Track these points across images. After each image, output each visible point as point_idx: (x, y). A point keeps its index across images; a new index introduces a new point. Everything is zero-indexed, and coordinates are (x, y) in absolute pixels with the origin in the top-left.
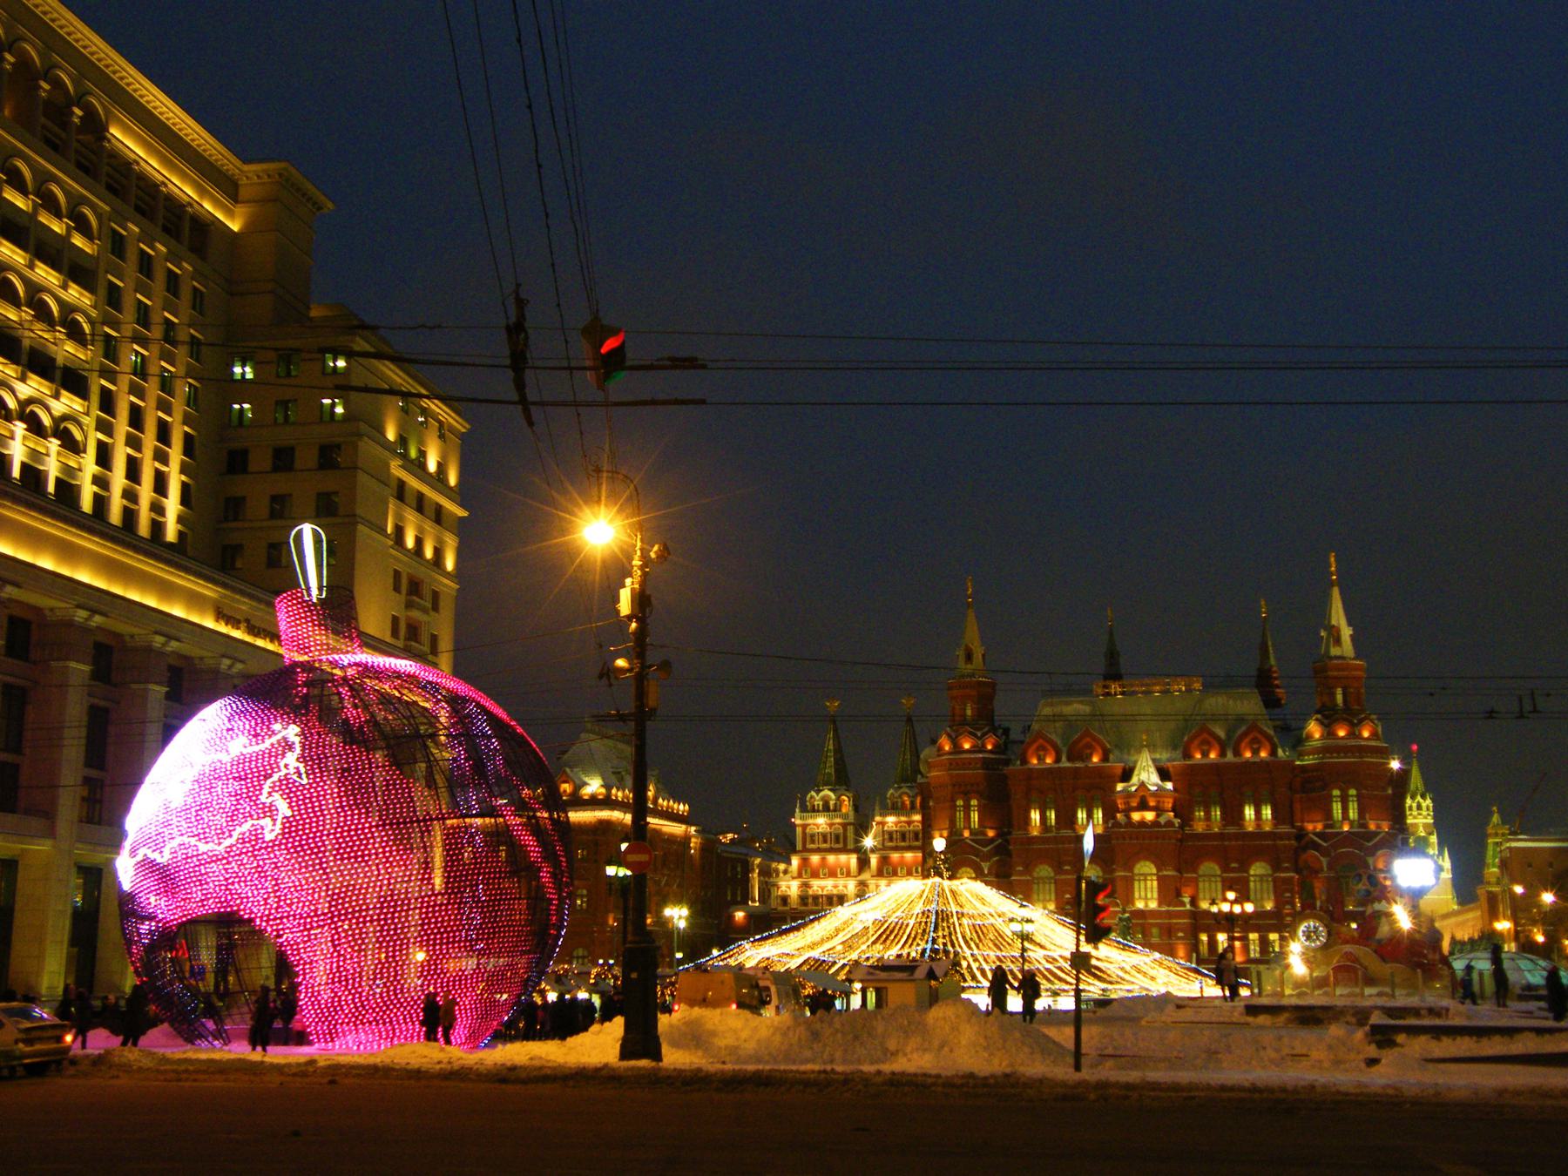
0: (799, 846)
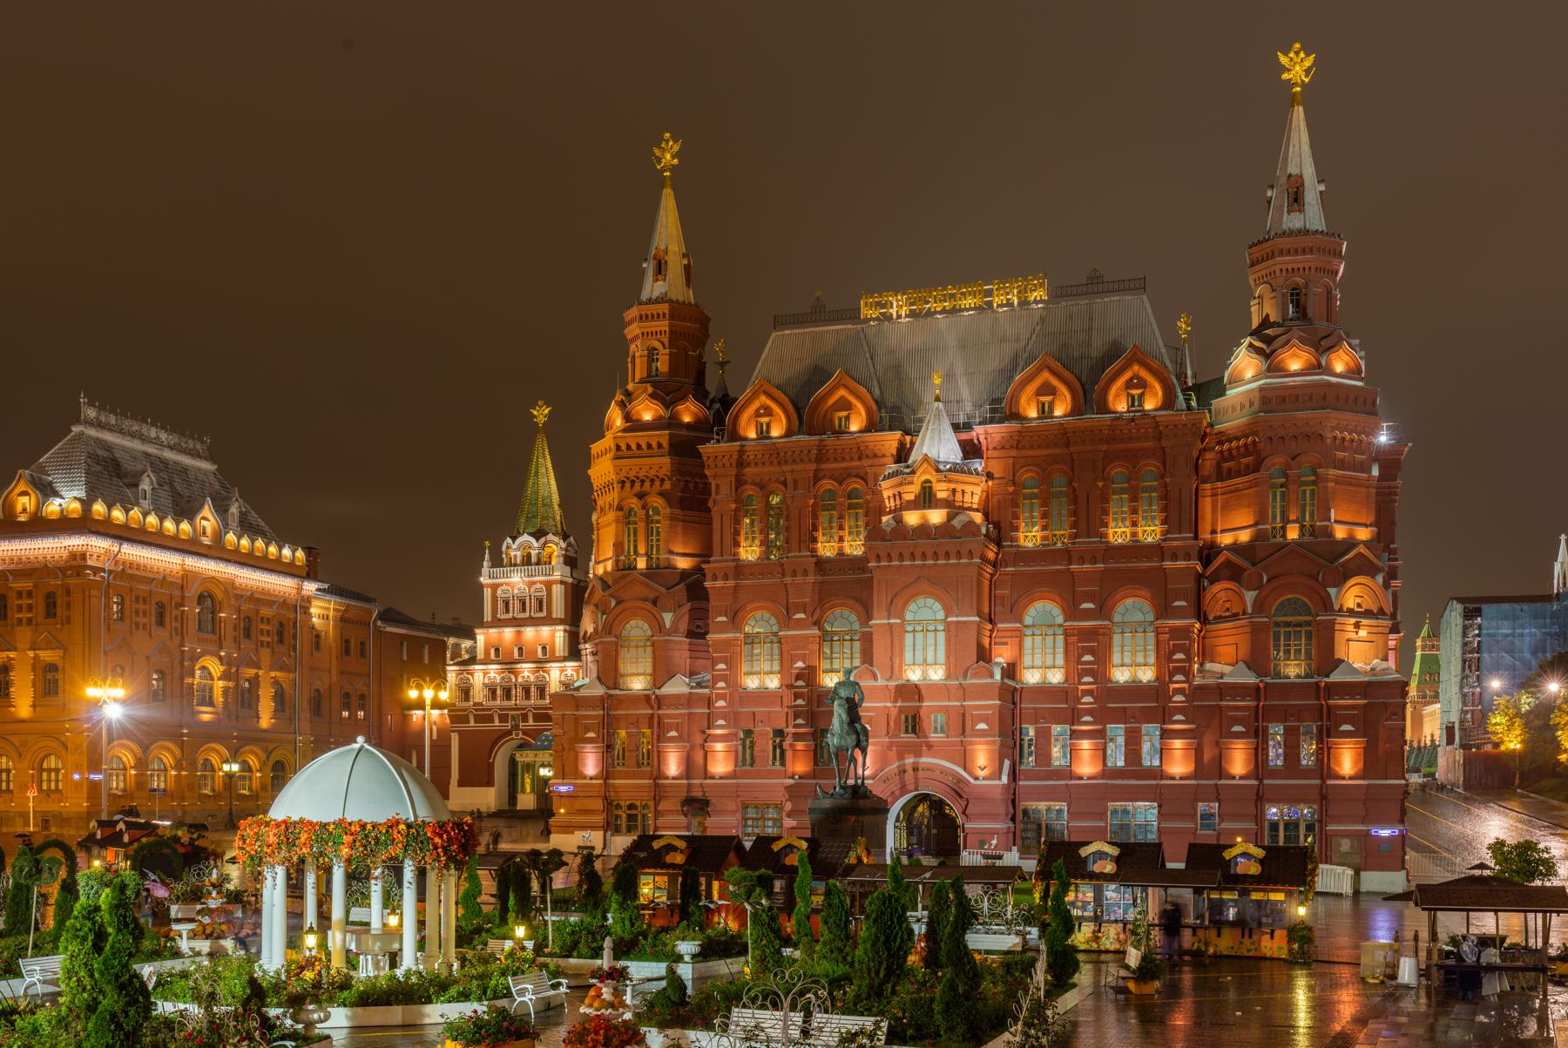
0: (488, 616)
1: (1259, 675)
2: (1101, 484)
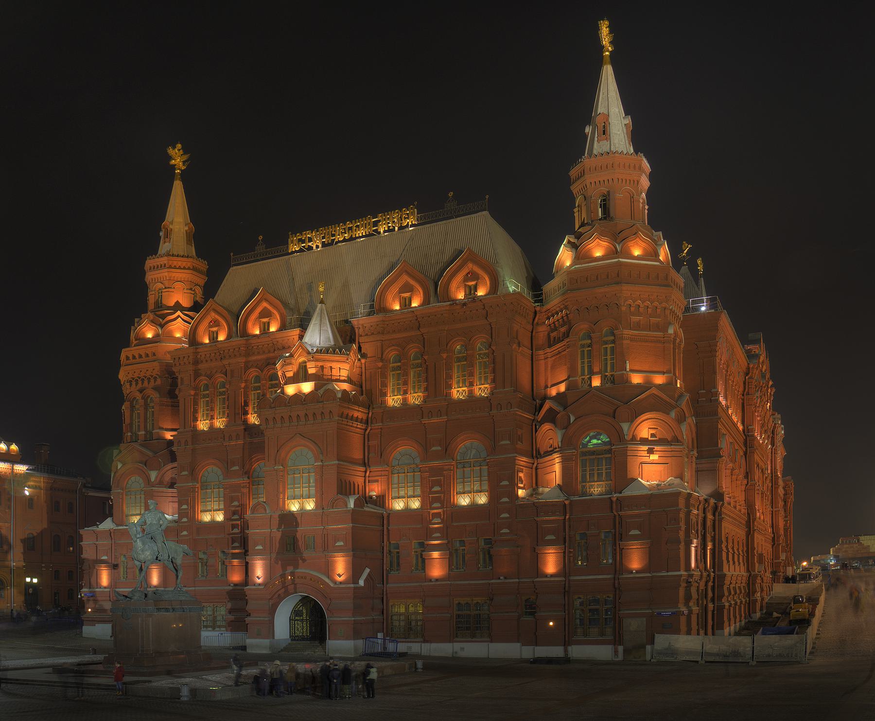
2: (445, 356)
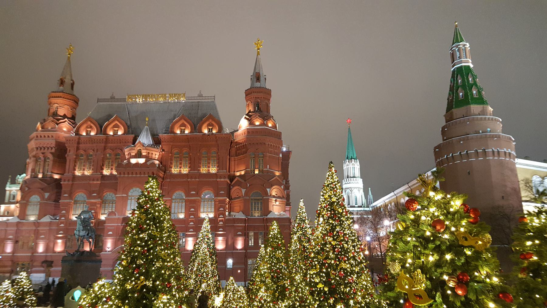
1: (246, 216)
